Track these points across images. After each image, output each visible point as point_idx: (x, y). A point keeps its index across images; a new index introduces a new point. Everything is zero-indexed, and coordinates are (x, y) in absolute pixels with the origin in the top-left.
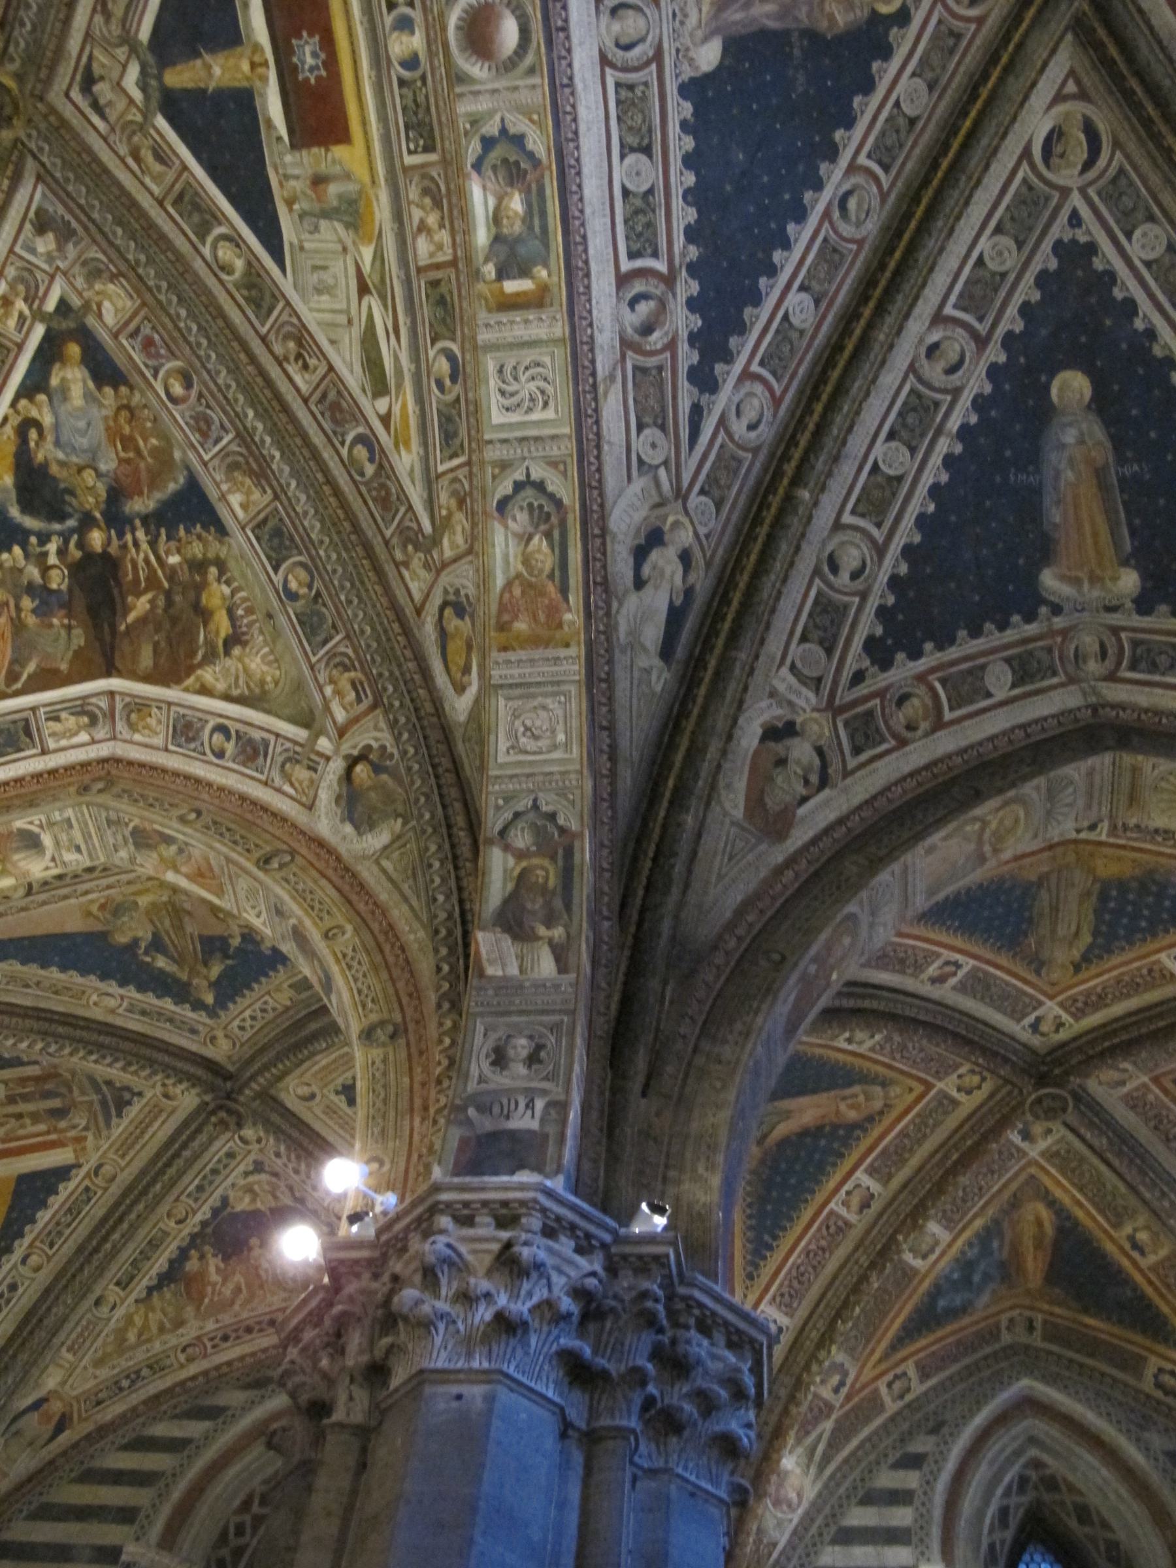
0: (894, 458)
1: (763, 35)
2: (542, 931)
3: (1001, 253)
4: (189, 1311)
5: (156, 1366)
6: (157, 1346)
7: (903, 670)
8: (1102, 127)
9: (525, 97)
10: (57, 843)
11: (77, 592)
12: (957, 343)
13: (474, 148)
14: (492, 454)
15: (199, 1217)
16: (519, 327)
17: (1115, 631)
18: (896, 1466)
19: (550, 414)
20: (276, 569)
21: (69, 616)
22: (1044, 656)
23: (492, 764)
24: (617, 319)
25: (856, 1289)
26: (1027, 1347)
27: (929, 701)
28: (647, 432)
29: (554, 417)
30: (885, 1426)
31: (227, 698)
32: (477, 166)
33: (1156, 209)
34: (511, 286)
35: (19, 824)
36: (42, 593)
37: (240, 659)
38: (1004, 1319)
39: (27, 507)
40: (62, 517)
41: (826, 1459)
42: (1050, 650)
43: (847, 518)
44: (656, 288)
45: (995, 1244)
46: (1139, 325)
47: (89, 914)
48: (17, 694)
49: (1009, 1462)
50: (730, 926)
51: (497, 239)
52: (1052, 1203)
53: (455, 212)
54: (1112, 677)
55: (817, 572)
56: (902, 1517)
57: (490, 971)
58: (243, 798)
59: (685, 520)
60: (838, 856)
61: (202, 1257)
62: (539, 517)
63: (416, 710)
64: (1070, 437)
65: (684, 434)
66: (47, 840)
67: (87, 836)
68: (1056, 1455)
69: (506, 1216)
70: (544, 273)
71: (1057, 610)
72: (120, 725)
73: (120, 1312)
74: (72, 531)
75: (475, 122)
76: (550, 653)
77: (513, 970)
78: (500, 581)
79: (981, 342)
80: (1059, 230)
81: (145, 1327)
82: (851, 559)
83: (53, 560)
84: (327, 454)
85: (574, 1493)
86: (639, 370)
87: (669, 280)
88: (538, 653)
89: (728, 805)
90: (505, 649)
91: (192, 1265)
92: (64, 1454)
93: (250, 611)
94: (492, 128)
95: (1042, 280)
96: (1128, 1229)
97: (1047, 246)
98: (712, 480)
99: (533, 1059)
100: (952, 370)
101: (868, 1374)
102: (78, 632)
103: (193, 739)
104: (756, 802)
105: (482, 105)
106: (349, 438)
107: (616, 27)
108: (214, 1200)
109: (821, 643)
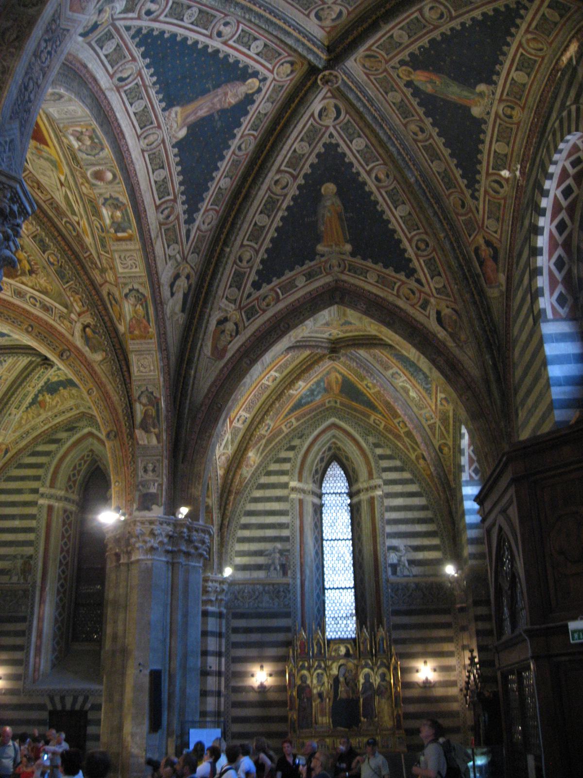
0: (262, 220)
1: (203, 119)
2: (152, 430)
3: (302, 148)
4: (42, 411)
5: (33, 429)
6: (33, 423)
7: (265, 288)
8: (341, 106)
9: (118, 189)
12: (287, 178)
13: (101, 201)
14: (121, 281)
15: (40, 385)
16: (124, 246)
17: (344, 260)
18: (287, 450)
19: (138, 270)
20: (44, 253)
22: (318, 270)
23: (133, 375)
24: (157, 219)
25: (271, 406)
26: (335, 408)
27: (274, 295)
28: (171, 247)
29: (140, 270)
30: (284, 437)
31: (33, 288)
32: (104, 204)
33: (362, 134)
34: (120, 235)
38: (327, 401)
41: (263, 450)
42: (320, 268)
43: (245, 243)
44: (169, 204)
45: (322, 384)
46: (354, 170)
49: (326, 443)
50: (207, 394)
51: (113, 222)
52: (340, 373)
53: (97, 213)
54: (342, 272)
55: (235, 262)
56: (287, 466)
57: (141, 442)
58: (47, 323)
59: (187, 265)
60: (241, 359)
61: (43, 395)
62: (138, 299)
63: (105, 323)
64: (328, 203)
65: (184, 240)
68: (341, 441)
69: (151, 522)
70: (130, 231)
71: (322, 256)
73: (18, 416)
75: (101, 195)
76: (147, 341)
77: (146, 442)
78: (128, 318)
79: (295, 178)
80: (325, 139)
81: (28, 418)
82: (247, 256)
84: (56, 220)
85: (170, 574)
86: (167, 230)
87: (175, 200)
88: (143, 341)
89: (206, 352)
90: (133, 339)
91: (40, 398)
92: (10, 460)
93: (36, 264)
94: (107, 196)
95: (318, 156)
96: (365, 382)
97: (320, 144)
98: (196, 247)
99: (154, 470)
100: (283, 188)
101: (278, 424)
104: (215, 347)
105: (103, 191)
106: (64, 220)
107: (146, 141)
108: (45, 379)
109: (236, 287)
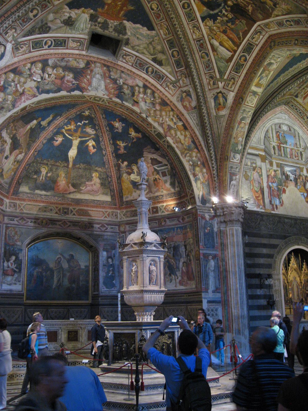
10: (275, 60)
11: (236, 15)
21: (239, 20)
35: (266, 63)
36: (230, 20)
37: (280, 7)
39: (213, 10)
40: (220, 5)
47: (288, 57)
48: (243, 40)
66: (272, 61)
67: (279, 55)
72: (266, 29)
74: (224, 6)
83: (226, 14)
102: (242, 21)
103: (283, 25)
